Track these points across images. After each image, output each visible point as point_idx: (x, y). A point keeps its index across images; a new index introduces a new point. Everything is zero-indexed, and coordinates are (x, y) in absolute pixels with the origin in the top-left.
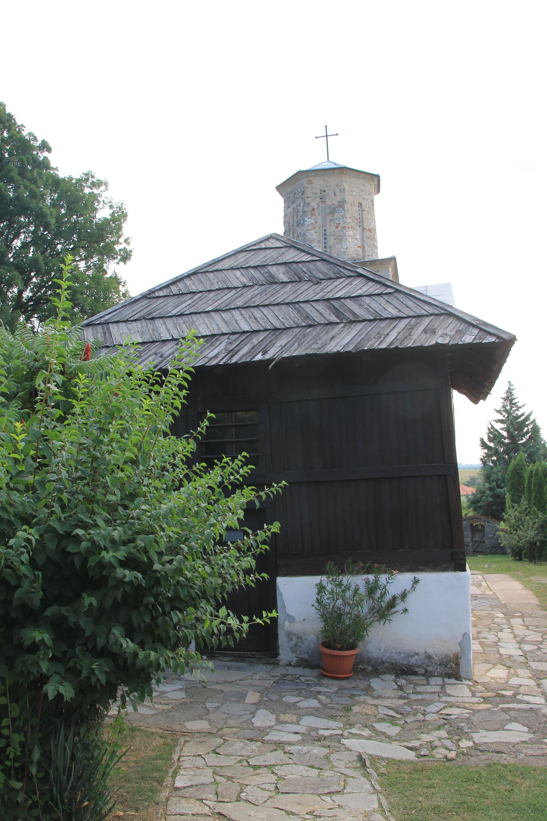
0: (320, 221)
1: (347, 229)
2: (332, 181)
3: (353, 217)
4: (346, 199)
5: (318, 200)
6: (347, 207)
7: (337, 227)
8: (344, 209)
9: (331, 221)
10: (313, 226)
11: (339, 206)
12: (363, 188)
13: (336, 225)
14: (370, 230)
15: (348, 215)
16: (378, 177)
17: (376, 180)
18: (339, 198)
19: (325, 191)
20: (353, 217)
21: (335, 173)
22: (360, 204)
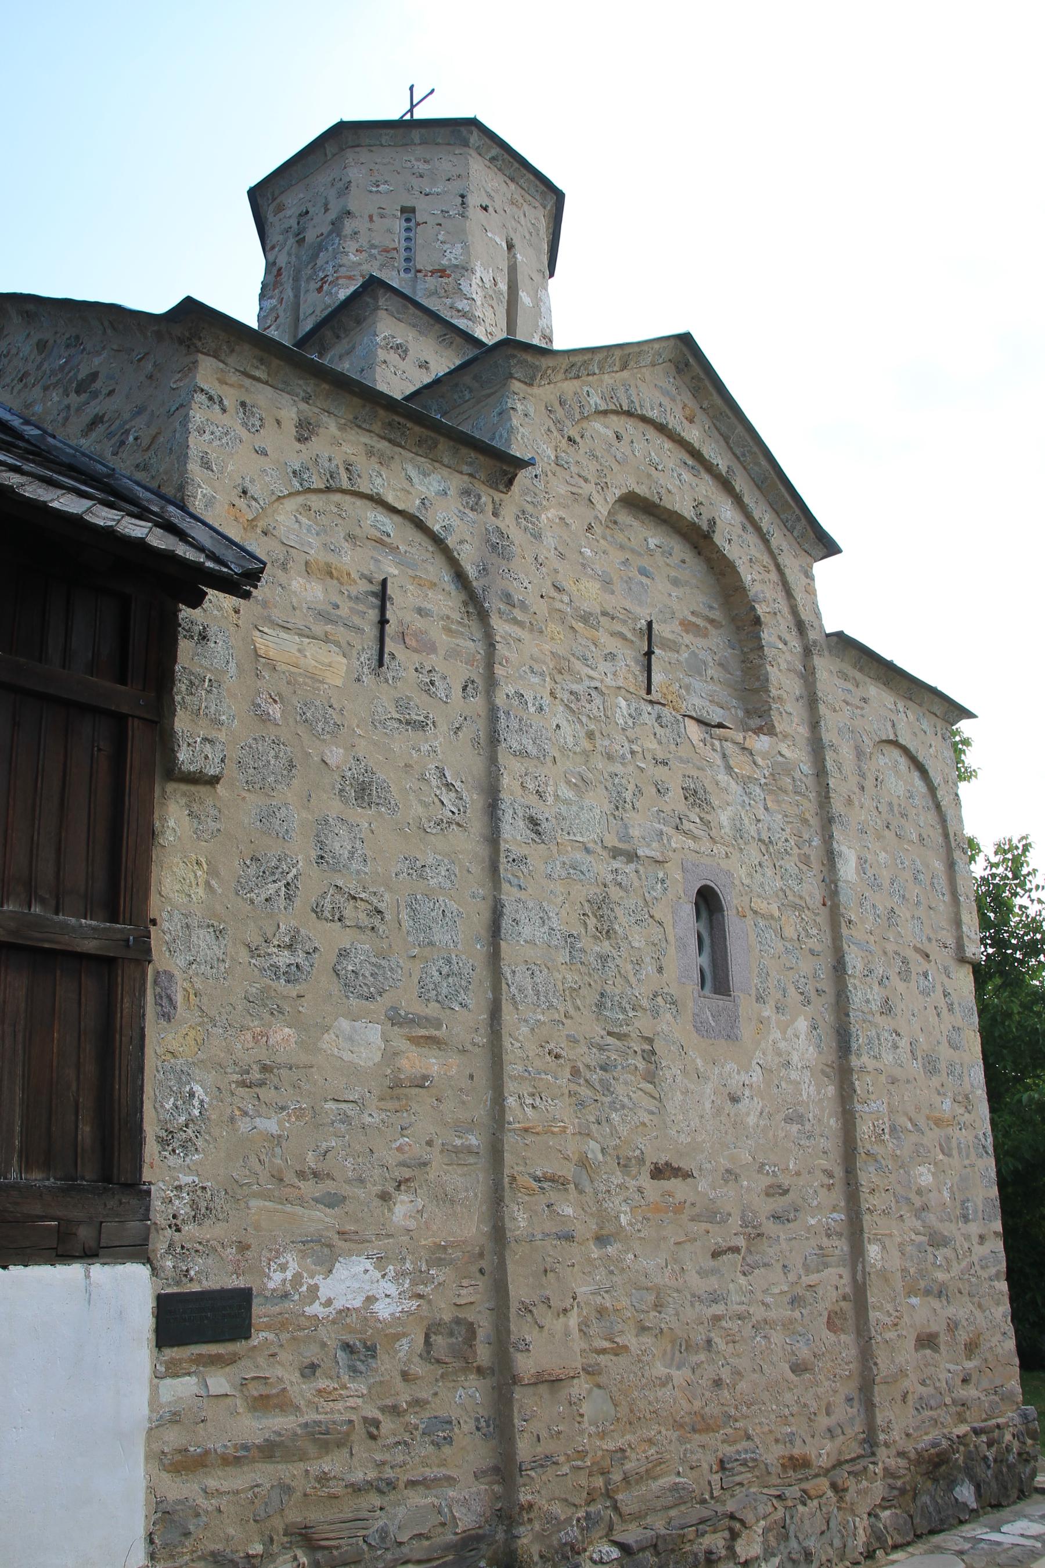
0: (289, 293)
1: (341, 281)
2: (322, 180)
3: (373, 246)
4: (351, 207)
5: (291, 241)
6: (349, 226)
7: (320, 290)
8: (339, 235)
9: (309, 279)
10: (274, 315)
11: (330, 233)
12: (422, 167)
13: (320, 284)
14: (442, 272)
15: (351, 246)
16: (473, 123)
17: (474, 138)
18: (332, 215)
19: (307, 212)
20: (373, 246)
21: (329, 156)
22: (408, 212)
